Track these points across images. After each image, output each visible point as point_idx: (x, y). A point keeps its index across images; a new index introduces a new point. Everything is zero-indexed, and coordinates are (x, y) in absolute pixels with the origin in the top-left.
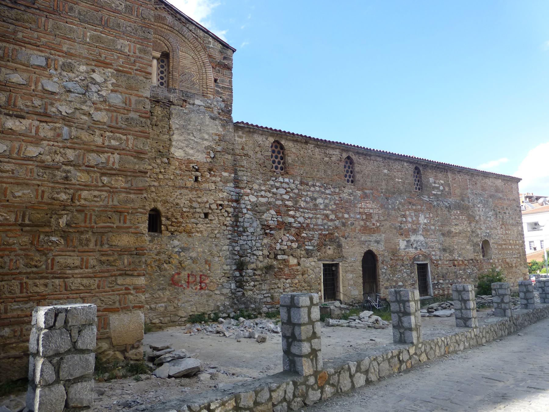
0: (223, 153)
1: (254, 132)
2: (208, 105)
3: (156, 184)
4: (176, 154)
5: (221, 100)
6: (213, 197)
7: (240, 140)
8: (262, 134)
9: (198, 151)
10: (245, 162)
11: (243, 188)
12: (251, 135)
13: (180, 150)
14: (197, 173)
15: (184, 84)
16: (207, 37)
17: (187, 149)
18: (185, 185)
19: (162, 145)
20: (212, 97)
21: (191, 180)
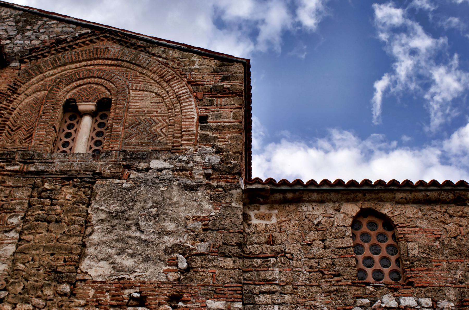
0: (210, 257)
1: (298, 201)
2: (179, 164)
4: (92, 273)
5: (214, 150)
7: (263, 222)
8: (322, 202)
9: (147, 259)
10: (277, 270)
12: (292, 207)
13: (103, 263)
15: (133, 141)
16: (187, 57)
17: (118, 259)
19: (62, 257)
20: (192, 149)
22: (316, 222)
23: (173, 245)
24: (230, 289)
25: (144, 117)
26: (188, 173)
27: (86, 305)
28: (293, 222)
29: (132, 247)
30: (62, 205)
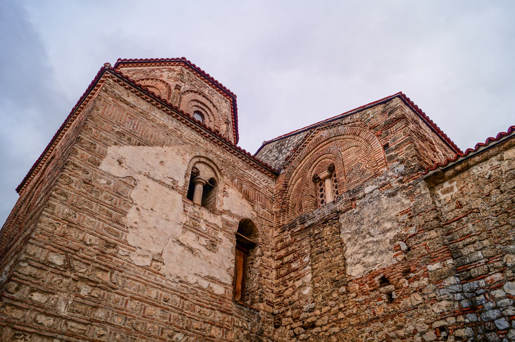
0: (419, 235)
2: (381, 183)
3: (336, 329)
4: (354, 274)
6: (423, 319)
7: (449, 195)
9: (381, 252)
10: (470, 225)
11: (482, 277)
14: (387, 287)
18: (374, 314)
19: (335, 271)
20: (385, 169)
21: (381, 302)
22: (487, 177)
23: (394, 237)
24: (440, 252)
25: (354, 164)
26: (388, 185)
27: (357, 296)
28: (470, 185)
29: (371, 249)
30: (326, 240)
